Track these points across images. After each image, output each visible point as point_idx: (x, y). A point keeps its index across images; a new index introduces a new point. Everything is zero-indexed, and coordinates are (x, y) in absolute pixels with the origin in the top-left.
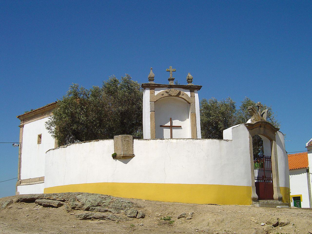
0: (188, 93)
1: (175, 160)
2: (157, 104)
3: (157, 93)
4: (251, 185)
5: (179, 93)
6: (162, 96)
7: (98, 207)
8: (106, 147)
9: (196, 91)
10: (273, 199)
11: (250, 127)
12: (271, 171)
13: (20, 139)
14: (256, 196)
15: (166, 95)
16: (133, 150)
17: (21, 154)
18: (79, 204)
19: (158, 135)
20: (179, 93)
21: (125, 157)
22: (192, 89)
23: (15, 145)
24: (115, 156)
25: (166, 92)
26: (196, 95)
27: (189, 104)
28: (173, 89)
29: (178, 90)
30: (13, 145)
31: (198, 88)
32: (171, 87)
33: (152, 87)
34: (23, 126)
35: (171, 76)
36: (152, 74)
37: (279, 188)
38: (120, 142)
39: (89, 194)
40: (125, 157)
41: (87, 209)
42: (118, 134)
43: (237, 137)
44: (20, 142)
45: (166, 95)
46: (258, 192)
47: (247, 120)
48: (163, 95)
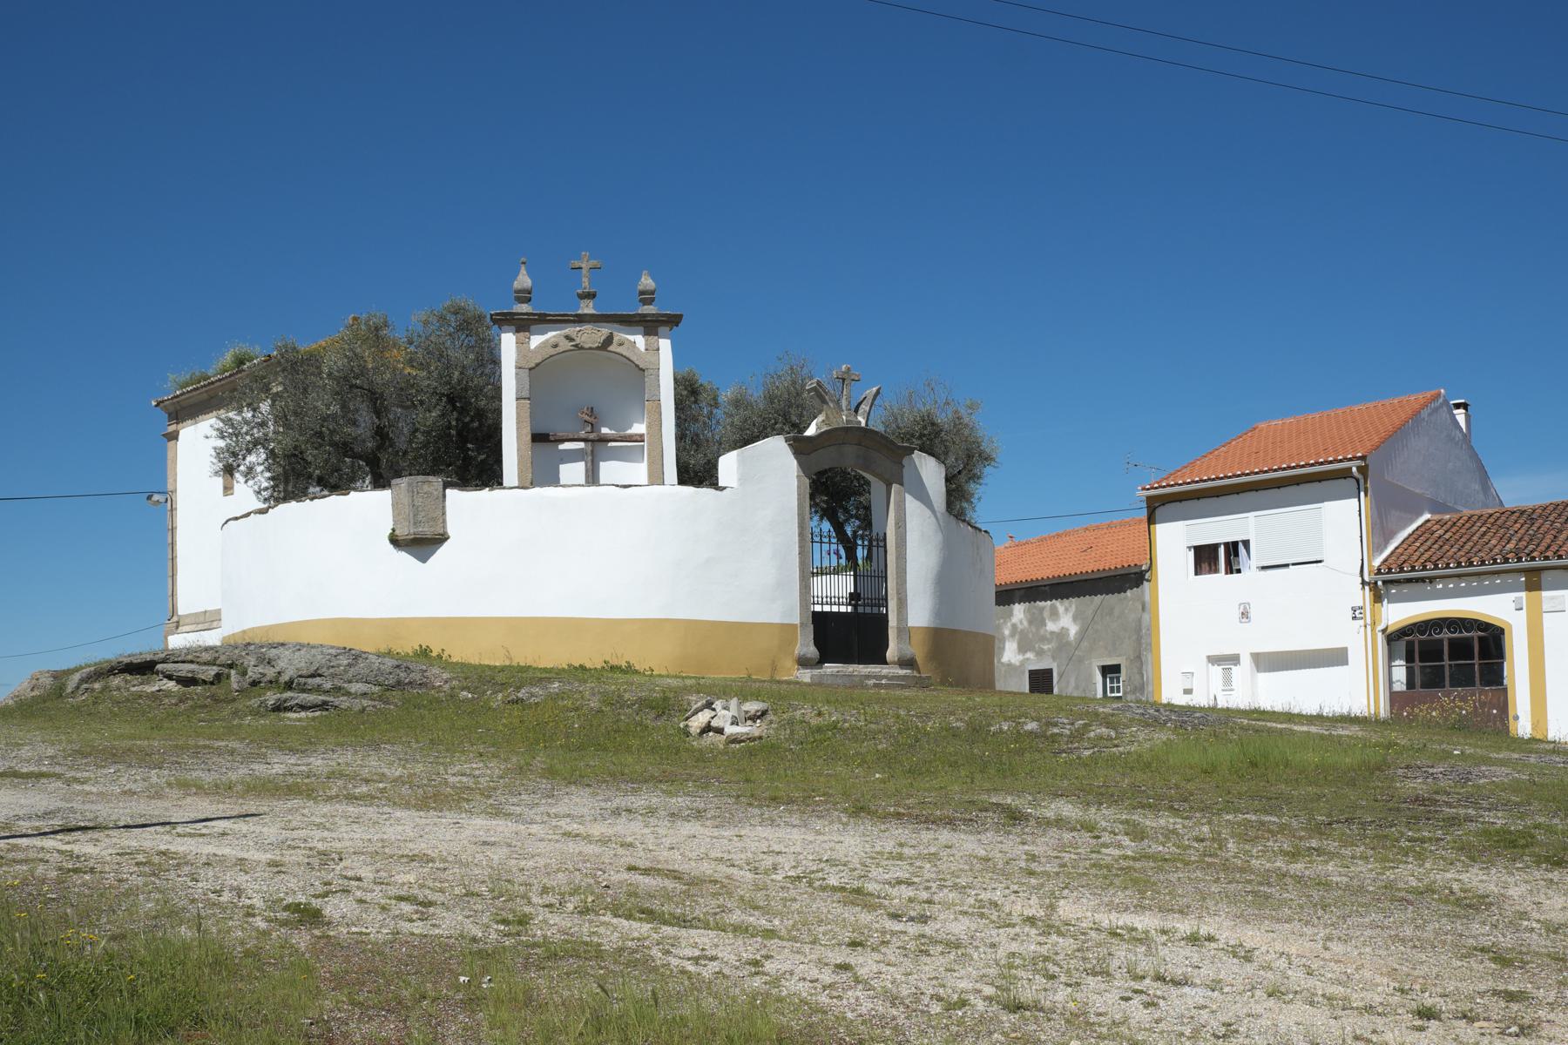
0: (640, 341)
1: (619, 549)
2: (536, 373)
3: (536, 341)
4: (796, 620)
5: (609, 340)
6: (553, 351)
7: (318, 680)
8: (369, 510)
9: (662, 329)
10: (882, 660)
11: (801, 447)
12: (884, 577)
13: (170, 481)
14: (812, 651)
15: (568, 345)
16: (444, 521)
17: (173, 529)
18: (270, 673)
19: (542, 474)
20: (609, 340)
21: (420, 542)
22: (650, 326)
23: (156, 497)
24: (395, 541)
25: (568, 338)
26: (665, 345)
27: (639, 375)
28: (587, 327)
29: (605, 330)
30: (149, 498)
31: (673, 321)
32: (581, 319)
33: (523, 325)
34: (174, 436)
35: (586, 285)
36: (524, 280)
37: (904, 631)
38: (406, 500)
39: (300, 647)
40: (420, 542)
41: (289, 686)
42: (398, 474)
43: (764, 476)
44: (170, 487)
45: (568, 345)
46: (818, 642)
47: (806, 428)
48: (556, 346)
